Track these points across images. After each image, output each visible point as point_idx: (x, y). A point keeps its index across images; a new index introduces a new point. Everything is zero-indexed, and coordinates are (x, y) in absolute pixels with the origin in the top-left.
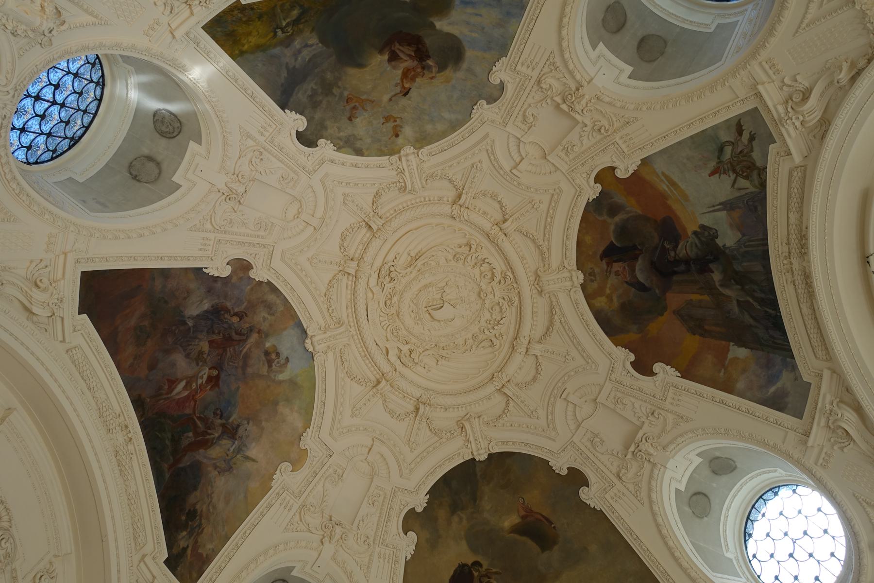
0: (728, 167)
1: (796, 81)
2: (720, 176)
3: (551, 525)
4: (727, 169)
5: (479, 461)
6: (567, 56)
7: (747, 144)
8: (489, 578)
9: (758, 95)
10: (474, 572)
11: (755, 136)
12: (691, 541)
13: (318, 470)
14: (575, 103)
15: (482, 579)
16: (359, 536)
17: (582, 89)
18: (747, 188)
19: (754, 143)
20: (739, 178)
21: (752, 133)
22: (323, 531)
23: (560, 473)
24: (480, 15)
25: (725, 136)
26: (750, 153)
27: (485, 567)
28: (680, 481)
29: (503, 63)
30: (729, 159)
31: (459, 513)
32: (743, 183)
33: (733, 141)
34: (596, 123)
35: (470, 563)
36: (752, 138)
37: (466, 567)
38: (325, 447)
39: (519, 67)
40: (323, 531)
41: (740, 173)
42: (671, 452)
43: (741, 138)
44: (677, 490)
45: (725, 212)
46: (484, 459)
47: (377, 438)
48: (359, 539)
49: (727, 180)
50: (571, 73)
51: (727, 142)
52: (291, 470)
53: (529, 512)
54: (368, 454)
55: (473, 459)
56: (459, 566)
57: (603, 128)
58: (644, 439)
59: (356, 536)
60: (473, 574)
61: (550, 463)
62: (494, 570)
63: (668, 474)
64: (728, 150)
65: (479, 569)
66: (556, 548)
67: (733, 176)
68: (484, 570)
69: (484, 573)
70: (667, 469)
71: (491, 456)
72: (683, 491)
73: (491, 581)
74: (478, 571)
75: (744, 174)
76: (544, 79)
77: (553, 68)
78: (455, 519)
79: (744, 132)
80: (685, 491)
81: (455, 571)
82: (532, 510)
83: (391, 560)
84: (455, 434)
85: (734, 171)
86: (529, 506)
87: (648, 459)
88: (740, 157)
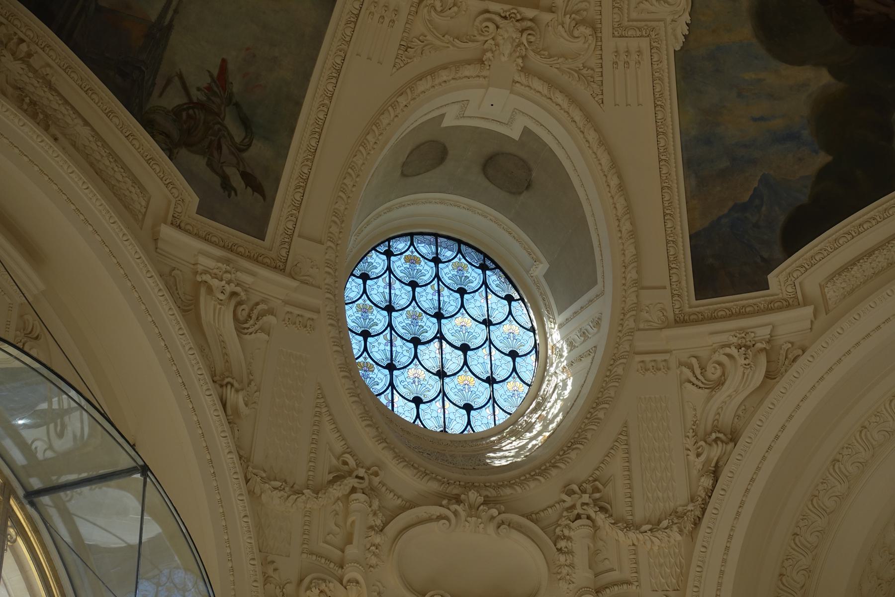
0: (213, 102)
1: (262, 329)
2: (211, 76)
4: (213, 98)
6: (577, 115)
7: (225, 168)
9: (280, 267)
11: (227, 193)
14: (519, 35)
17: (517, 65)
18: (161, 95)
19: (217, 180)
20: (185, 100)
21: (233, 193)
24: (755, 120)
25: (259, 150)
26: (209, 159)
29: (676, 38)
30: (223, 119)
32: (173, 99)
33: (245, 155)
34: (455, 9)
36: (226, 184)
39: (644, 44)
41: (191, 112)
43: (239, 171)
45: (153, 21)
49: (198, 81)
50: (551, 83)
51: (249, 145)
57: (439, 9)
64: (237, 133)
67: (196, 95)
75: (184, 114)
76: (589, 45)
77: (584, 72)
79: (243, 185)
85: (201, 105)
88: (213, 138)
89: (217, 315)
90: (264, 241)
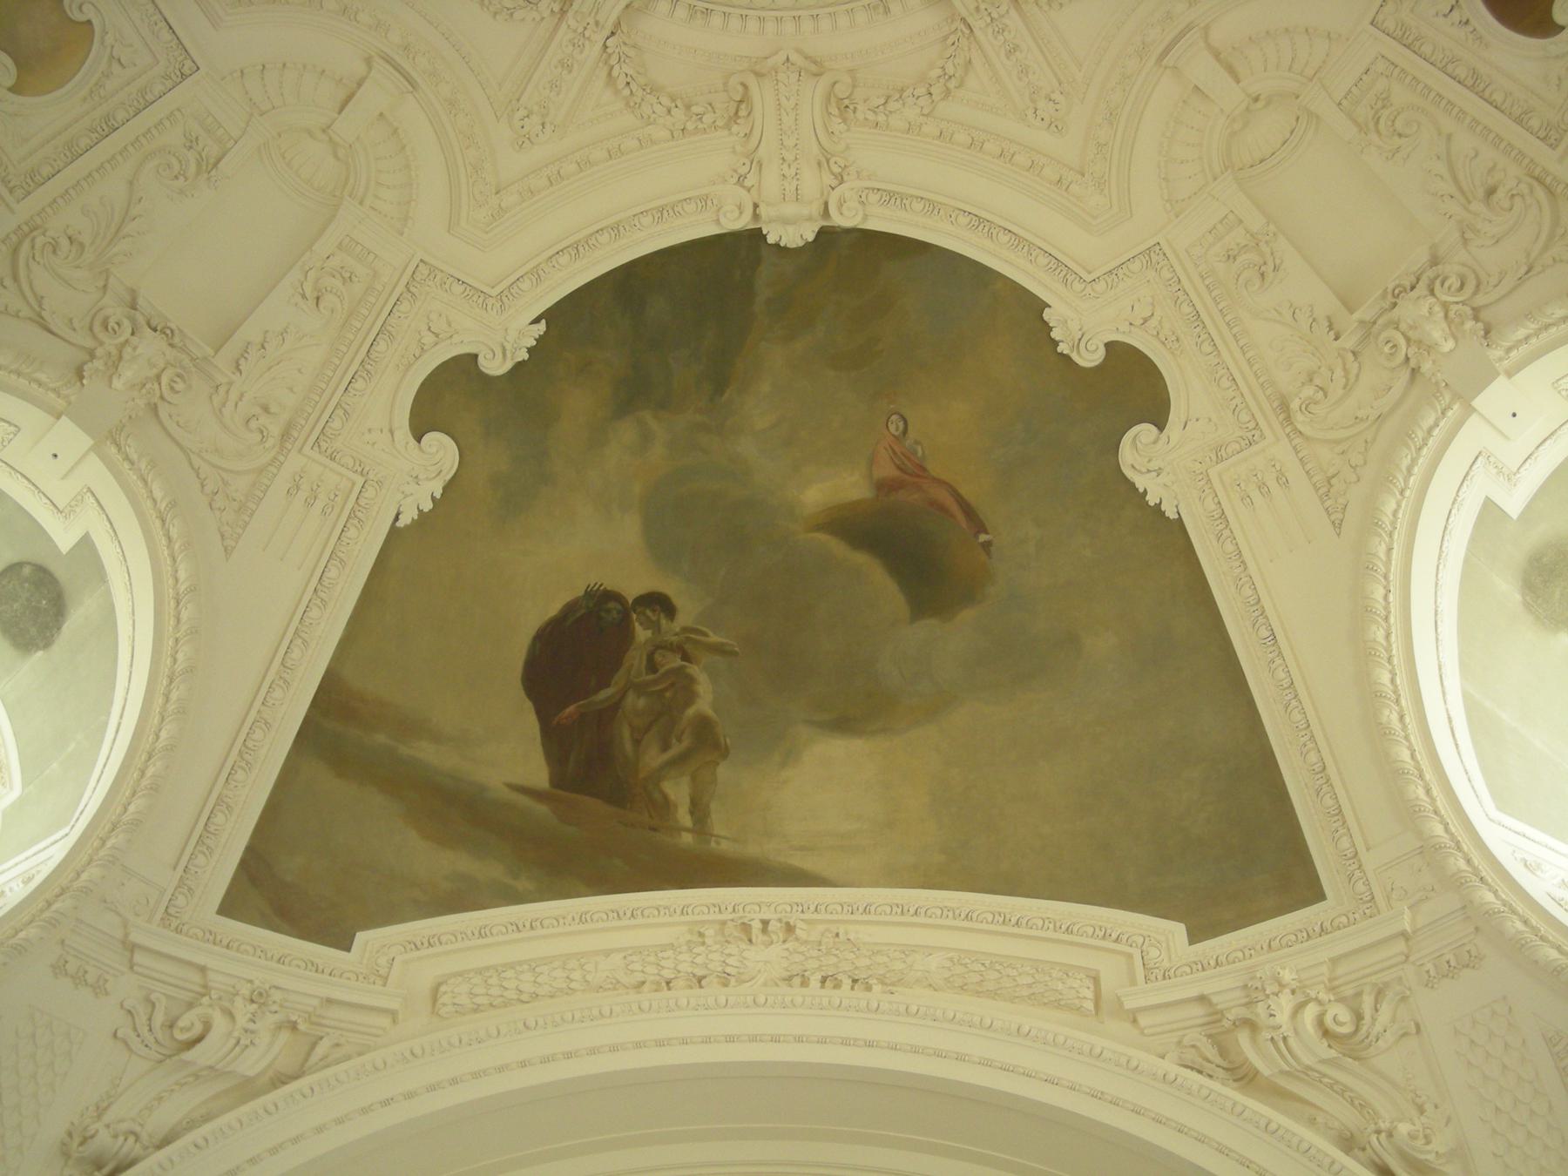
3: (976, 535)
5: (777, 245)
8: (686, 657)
10: (638, 628)
12: (1466, 697)
13: (121, 115)
15: (658, 657)
16: (233, 396)
22: (95, 337)
23: (1075, 357)
27: (684, 618)
28: (1511, 477)
31: (647, 415)
35: (632, 590)
37: (611, 605)
38: (166, 35)
40: (95, 337)
42: (1509, 350)
44: (1489, 507)
46: (801, 243)
47: (388, 60)
48: (230, 405)
52: (10, 82)
53: (913, 472)
54: (340, 112)
55: (756, 236)
56: (588, 594)
58: (1422, 285)
59: (222, 390)
60: (634, 628)
61: (1047, 315)
62: (714, 638)
63: (1471, 437)
65: (659, 620)
66: (967, 615)
68: (678, 629)
69: (674, 639)
70: (1474, 418)
71: (827, 237)
72: (1515, 517)
73: (688, 670)
74: (657, 628)
78: (626, 432)
80: (1519, 519)
81: (569, 608)
82: (924, 469)
83: (337, 510)
84: (708, 119)
86: (920, 453)
87: (1413, 363)
89: (1289, 1057)
90: (1190, 945)
